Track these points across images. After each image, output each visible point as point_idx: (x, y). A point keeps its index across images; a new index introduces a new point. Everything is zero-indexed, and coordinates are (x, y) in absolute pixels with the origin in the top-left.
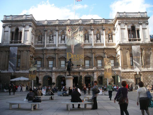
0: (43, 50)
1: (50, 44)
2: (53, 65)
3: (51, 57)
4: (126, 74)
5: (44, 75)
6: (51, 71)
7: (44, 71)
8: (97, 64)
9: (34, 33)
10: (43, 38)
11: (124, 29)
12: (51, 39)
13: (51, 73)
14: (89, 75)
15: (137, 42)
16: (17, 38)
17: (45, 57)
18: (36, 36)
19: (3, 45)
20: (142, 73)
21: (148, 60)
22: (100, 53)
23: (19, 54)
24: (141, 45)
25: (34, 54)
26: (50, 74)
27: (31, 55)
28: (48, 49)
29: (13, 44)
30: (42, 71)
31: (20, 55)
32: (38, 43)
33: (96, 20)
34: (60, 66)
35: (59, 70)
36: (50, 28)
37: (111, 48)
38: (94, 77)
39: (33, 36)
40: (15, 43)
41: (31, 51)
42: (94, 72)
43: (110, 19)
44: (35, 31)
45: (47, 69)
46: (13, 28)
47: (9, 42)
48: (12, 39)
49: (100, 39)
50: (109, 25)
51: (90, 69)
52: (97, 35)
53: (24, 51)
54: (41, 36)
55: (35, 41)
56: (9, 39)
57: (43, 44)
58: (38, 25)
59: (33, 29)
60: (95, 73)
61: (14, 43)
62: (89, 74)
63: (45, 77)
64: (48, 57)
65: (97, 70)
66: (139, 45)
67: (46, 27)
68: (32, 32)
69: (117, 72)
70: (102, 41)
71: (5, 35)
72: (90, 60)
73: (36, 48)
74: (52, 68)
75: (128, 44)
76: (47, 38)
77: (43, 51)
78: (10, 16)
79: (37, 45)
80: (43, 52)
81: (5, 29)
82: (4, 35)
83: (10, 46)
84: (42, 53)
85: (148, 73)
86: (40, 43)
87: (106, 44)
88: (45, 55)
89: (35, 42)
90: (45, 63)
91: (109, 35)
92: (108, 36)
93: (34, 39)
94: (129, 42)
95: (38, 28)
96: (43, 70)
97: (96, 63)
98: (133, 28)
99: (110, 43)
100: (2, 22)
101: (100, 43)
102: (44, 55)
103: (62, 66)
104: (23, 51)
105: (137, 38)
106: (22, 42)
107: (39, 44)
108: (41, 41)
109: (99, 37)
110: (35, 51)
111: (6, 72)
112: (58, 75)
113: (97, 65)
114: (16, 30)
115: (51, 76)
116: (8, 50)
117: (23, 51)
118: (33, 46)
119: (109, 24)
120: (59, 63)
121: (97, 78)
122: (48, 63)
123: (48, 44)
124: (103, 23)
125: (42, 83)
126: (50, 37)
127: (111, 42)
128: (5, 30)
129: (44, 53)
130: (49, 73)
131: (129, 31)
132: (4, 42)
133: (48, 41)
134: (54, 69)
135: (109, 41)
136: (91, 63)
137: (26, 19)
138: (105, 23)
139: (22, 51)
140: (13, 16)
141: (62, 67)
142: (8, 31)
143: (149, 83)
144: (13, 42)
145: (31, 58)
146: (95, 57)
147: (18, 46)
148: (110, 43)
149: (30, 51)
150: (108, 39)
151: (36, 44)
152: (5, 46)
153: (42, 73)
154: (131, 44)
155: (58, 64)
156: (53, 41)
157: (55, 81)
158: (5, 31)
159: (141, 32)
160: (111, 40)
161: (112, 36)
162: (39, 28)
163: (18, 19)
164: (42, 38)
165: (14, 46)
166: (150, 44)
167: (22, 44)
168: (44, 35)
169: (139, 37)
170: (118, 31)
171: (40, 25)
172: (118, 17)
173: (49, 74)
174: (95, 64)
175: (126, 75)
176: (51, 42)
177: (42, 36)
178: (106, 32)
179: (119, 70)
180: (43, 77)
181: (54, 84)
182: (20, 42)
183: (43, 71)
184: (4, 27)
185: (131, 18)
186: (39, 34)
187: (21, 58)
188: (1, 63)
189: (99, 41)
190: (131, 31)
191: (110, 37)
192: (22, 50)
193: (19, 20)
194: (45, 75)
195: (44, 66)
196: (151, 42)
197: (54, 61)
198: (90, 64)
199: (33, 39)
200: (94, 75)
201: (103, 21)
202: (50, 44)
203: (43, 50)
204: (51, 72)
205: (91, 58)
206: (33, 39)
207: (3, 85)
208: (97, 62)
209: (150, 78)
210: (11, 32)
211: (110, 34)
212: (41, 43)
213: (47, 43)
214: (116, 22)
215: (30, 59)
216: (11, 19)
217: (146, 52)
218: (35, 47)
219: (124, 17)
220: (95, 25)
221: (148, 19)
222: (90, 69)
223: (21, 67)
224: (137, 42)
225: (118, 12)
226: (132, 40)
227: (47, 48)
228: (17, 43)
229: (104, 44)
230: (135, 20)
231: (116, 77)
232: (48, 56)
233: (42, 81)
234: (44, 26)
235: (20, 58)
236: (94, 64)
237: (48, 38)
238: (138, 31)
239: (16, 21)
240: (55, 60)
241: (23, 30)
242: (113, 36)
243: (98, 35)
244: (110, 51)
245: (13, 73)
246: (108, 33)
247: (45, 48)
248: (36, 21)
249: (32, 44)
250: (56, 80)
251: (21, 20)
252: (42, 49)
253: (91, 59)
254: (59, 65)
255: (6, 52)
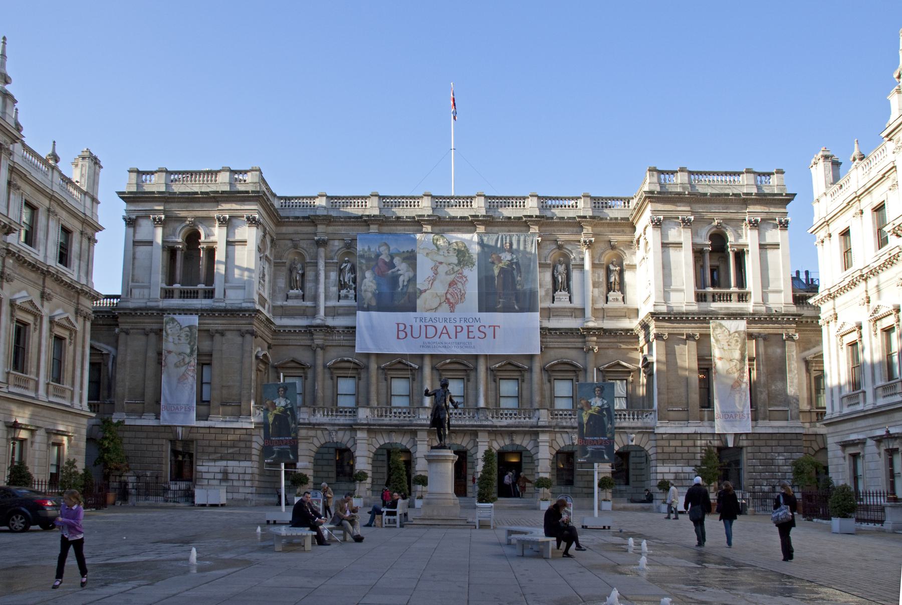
0: (312, 329)
1: (343, 303)
2: (356, 395)
3: (348, 361)
4: (678, 443)
5: (320, 439)
6: (351, 425)
7: (319, 424)
8: (553, 398)
9: (268, 253)
10: (310, 275)
11: (678, 245)
12: (346, 280)
13: (348, 433)
14: (513, 445)
15: (734, 305)
16: (191, 277)
17: (320, 362)
18: (278, 265)
19: (131, 305)
20: (749, 443)
21: (779, 385)
22: (567, 350)
23: (206, 345)
24: (753, 318)
25: (269, 347)
26: (346, 438)
27: (261, 351)
28: (334, 327)
29: (176, 302)
30: (309, 424)
31: (212, 350)
32: (287, 297)
33: (551, 198)
34: (389, 402)
35: (386, 420)
36: (342, 230)
37: (617, 330)
38: (540, 456)
39: (267, 266)
40: (184, 295)
41: (259, 333)
42: (536, 434)
43: (618, 199)
44: (272, 241)
45: (332, 415)
46: (175, 230)
47: (157, 293)
48: (171, 278)
49: (568, 288)
50: (609, 225)
51: (522, 420)
52: (554, 268)
53: (229, 335)
54: (299, 266)
55: (274, 291)
56: (158, 279)
57: (309, 304)
58: (288, 218)
59: (264, 236)
60: (543, 437)
61: (180, 297)
62: (518, 441)
63: (322, 446)
64: (335, 363)
65: (554, 423)
66: (742, 319)
67: (321, 228)
68: (259, 250)
69: (639, 433)
70: (575, 298)
71: (137, 263)
72: (523, 381)
73: (278, 322)
74: (354, 411)
75: (693, 314)
76: (326, 277)
77: (311, 334)
78: (156, 172)
79: (282, 307)
80: (312, 340)
81: (135, 232)
82: (134, 258)
83: (162, 311)
84: (308, 343)
85: (774, 443)
86: (296, 297)
87: (595, 310)
88: (320, 352)
89: (273, 295)
90: (319, 386)
91: (608, 270)
92: (602, 273)
93: (270, 282)
94: (695, 307)
95: (284, 229)
96: (313, 420)
97: (547, 393)
98: (719, 240)
99: (610, 305)
100: (123, 198)
101: (568, 305)
102: (315, 352)
103: (396, 402)
104: (222, 333)
105: (733, 289)
106: (218, 294)
107: (290, 303)
108: (302, 288)
109: (564, 276)
110: (275, 333)
111: (148, 421)
112: (382, 443)
113: (552, 403)
114: (187, 238)
115: (349, 446)
116: (155, 326)
117: (222, 333)
118: (265, 312)
119: (611, 219)
120: (383, 391)
121: (549, 456)
122: (335, 386)
123: (333, 303)
124: (585, 217)
125: (310, 473)
126: (341, 271)
127: (617, 300)
128: (139, 237)
129: (318, 346)
130: (341, 434)
131: (698, 253)
132: (136, 292)
133: (334, 289)
134: (364, 414)
135: (610, 298)
136: (525, 394)
137: (234, 189)
138: (591, 217)
139: (217, 331)
140: (172, 173)
141: (399, 408)
142: (150, 243)
143: (774, 487)
144: (177, 294)
145: (258, 364)
146: (544, 369)
147: (202, 310)
148: (610, 305)
149: (253, 334)
150: (604, 289)
151: (279, 303)
152: (140, 309)
153: (312, 433)
154: (707, 313)
155: (378, 393)
156: (355, 289)
157: (370, 467)
158: (136, 243)
159: (753, 261)
160: (618, 295)
161: (621, 273)
162: (291, 229)
163: (196, 188)
164: (303, 275)
165: (183, 310)
166: (792, 315)
167: (219, 301)
168: (316, 264)
169: (741, 282)
170: (651, 255)
171: (298, 218)
172: (652, 192)
173: (342, 438)
174: (542, 396)
175: (679, 450)
176: (346, 297)
177: (303, 268)
178: (597, 257)
179: (646, 428)
180: (315, 449)
181: (362, 476)
182: (210, 294)
183: (314, 425)
184: (131, 222)
185: (712, 195)
186: (289, 257)
187: (215, 362)
188: (127, 383)
189: (562, 295)
190: (707, 256)
191: (612, 279)
192: (220, 328)
193: (202, 193)
194: (323, 442)
195: (314, 401)
196: (794, 309)
197: (414, 380)
198: (519, 397)
199: (267, 278)
200: (537, 446)
201: (581, 203)
202: (343, 303)
203: (309, 331)
204: (352, 428)
205: (526, 370)
206: (267, 278)
207: (138, 477)
208: (552, 389)
209: (781, 462)
210: (163, 247)
211: (612, 267)
212: (303, 298)
213: (326, 299)
214: (640, 210)
215: (254, 368)
216: (163, 189)
217: (770, 350)
218: (274, 315)
219: (679, 190)
220: (548, 225)
221: (788, 201)
222: (522, 420)
223: (214, 403)
224: (734, 305)
225: (653, 166)
226: (710, 298)
227: (330, 322)
228: (194, 295)
229: (583, 310)
230: (727, 208)
231: (632, 454)
232: (332, 356)
233: (311, 466)
234: (313, 220)
235: (209, 364)
236: (537, 399)
237: (333, 275)
238: (740, 256)
239: (188, 198)
240: (363, 375)
241: (218, 235)
242: (628, 276)
243: (561, 268)
244: (612, 340)
245: (180, 430)
246: (604, 260)
247: (318, 322)
248: (274, 195)
249: (262, 301)
250: (370, 461)
251: (207, 193)
252: (307, 327)
253: (527, 375)
254: (383, 399)
255: (147, 335)
